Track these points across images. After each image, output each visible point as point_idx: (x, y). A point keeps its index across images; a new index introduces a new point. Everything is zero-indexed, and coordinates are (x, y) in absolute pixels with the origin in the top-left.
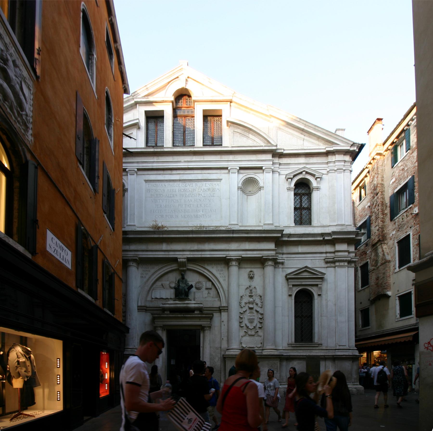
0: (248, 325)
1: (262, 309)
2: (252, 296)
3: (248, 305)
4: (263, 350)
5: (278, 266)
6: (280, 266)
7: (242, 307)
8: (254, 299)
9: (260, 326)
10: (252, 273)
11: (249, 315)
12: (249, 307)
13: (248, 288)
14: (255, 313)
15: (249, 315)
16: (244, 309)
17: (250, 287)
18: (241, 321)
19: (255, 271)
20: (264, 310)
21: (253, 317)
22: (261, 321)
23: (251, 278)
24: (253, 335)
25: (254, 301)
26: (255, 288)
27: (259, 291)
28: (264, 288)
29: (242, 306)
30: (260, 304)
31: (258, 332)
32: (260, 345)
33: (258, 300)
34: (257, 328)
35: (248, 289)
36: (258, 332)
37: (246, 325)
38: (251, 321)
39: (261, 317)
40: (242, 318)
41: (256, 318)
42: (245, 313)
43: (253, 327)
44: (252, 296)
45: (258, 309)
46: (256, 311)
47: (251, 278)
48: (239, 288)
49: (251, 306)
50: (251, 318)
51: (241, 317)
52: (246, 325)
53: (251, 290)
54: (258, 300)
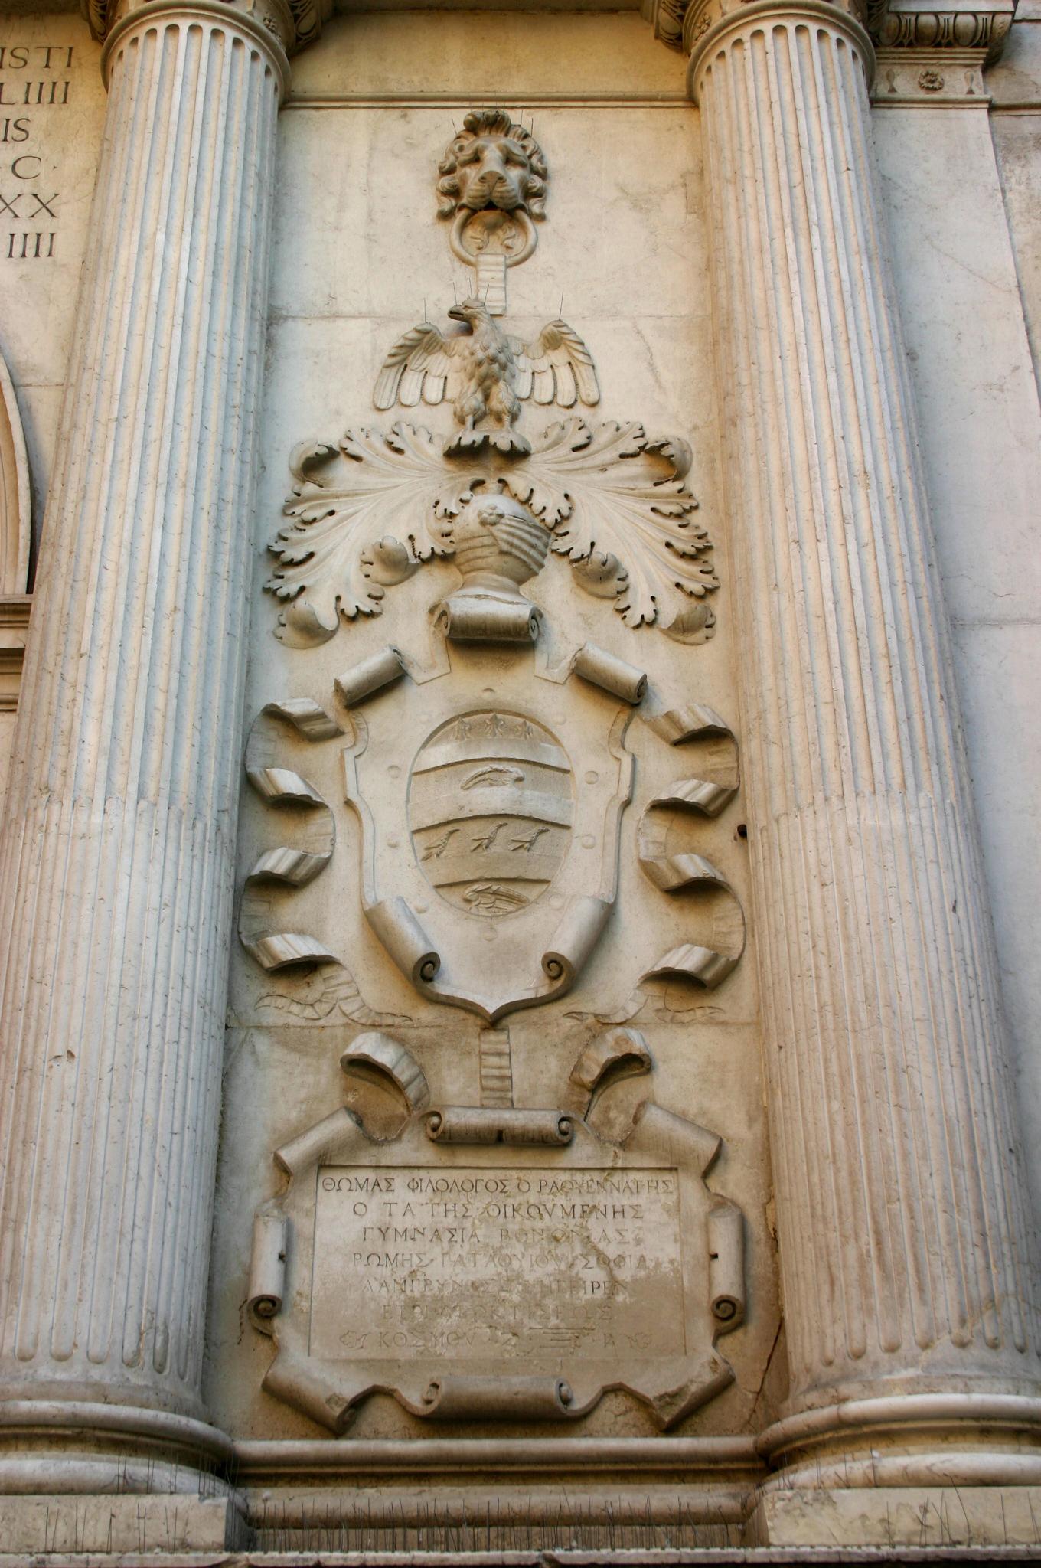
0: (439, 928)
1: (708, 656)
2: (516, 456)
3: (426, 587)
4: (771, 1460)
5: (932, 83)
6: (959, 80)
7: (313, 633)
8: (548, 501)
9: (687, 960)
10: (492, 149)
11: (442, 753)
12: (439, 613)
13: (424, 342)
14: (576, 725)
15: (442, 753)
16: (355, 659)
17: (465, 321)
18: (277, 861)
19: (554, 134)
20: (738, 672)
21: (537, 801)
22: (693, 867)
23: (494, 205)
24: (552, 1143)
25: (557, 527)
26: (554, 340)
27: (639, 387)
28: (718, 336)
29: (321, 607)
30: (653, 578)
31: (632, 1064)
32: (695, 1364)
33: (614, 519)
34: (619, 984)
35: (438, 363)
36: (632, 1064)
37: (376, 927)
38: (495, 862)
39: (699, 793)
40: (300, 806)
41: (588, 809)
42: (380, 717)
43: (529, 983)
44: (516, 456)
45: (629, 659)
46: (590, 681)
47: (494, 205)
48: (269, 342)
49: (491, 604)
50: (494, 798)
51: (289, 782)
52: (376, 927)
53: (490, 373)
54: (614, 519)
